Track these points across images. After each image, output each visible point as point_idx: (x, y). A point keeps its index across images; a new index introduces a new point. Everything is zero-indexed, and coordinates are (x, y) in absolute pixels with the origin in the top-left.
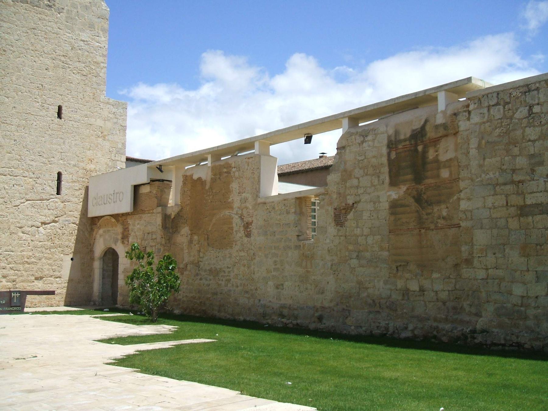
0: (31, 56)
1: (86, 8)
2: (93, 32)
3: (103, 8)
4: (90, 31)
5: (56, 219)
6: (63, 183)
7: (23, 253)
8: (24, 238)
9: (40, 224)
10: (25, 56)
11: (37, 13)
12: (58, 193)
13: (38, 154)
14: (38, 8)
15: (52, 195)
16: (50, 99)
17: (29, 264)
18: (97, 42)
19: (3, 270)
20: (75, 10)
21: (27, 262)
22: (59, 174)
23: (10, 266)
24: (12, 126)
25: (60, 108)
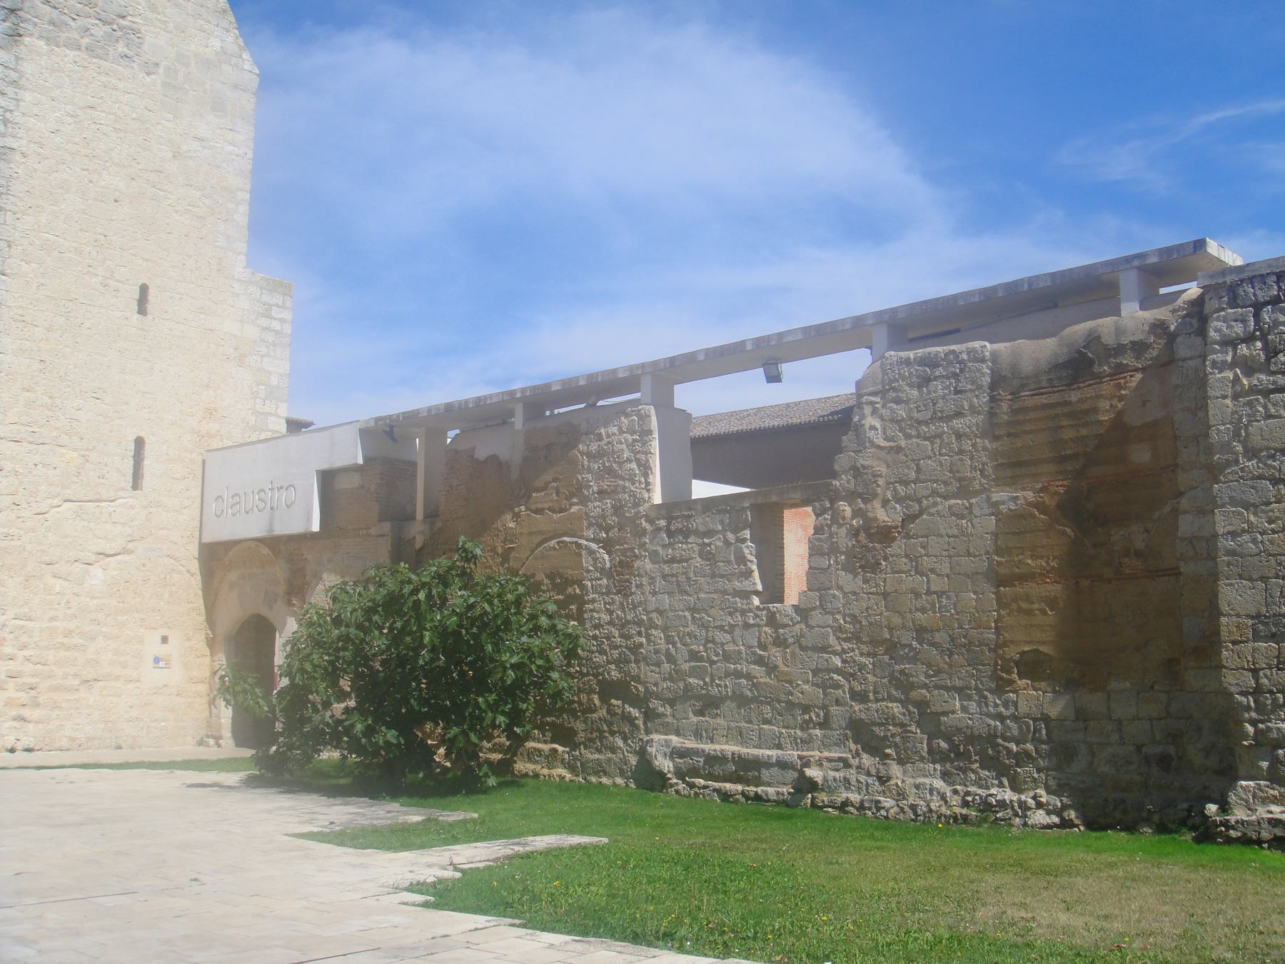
0: (84, 170)
5: (130, 546)
6: (146, 462)
7: (54, 623)
8: (57, 589)
9: (93, 557)
10: (71, 169)
12: (136, 485)
13: (95, 395)
14: (102, 62)
16: (123, 269)
17: (68, 649)
19: (7, 662)
21: (63, 644)
22: (140, 443)
23: (27, 653)
24: (36, 329)
25: (144, 289)
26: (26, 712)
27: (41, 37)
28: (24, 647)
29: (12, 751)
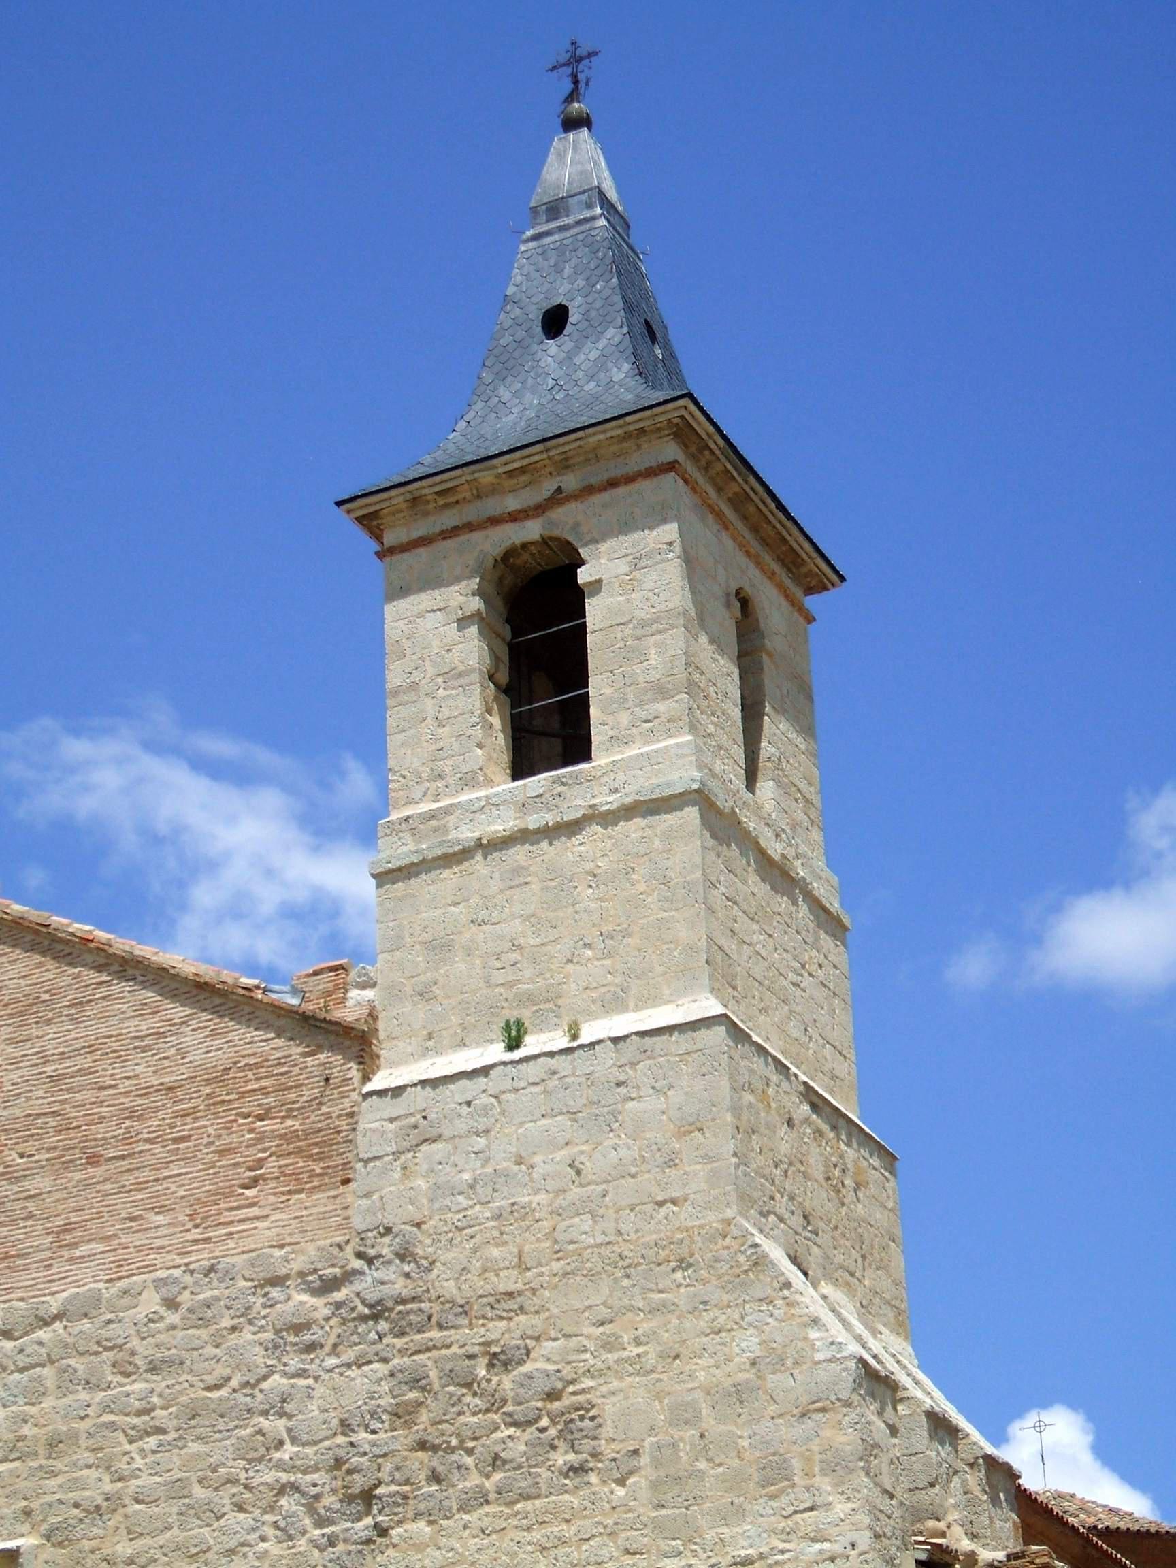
1: (740, 1393)
2: (784, 1500)
3: (819, 1356)
4: (772, 1497)
11: (529, 1529)
18: (814, 1540)
20: (693, 1432)
27: (418, 1515)
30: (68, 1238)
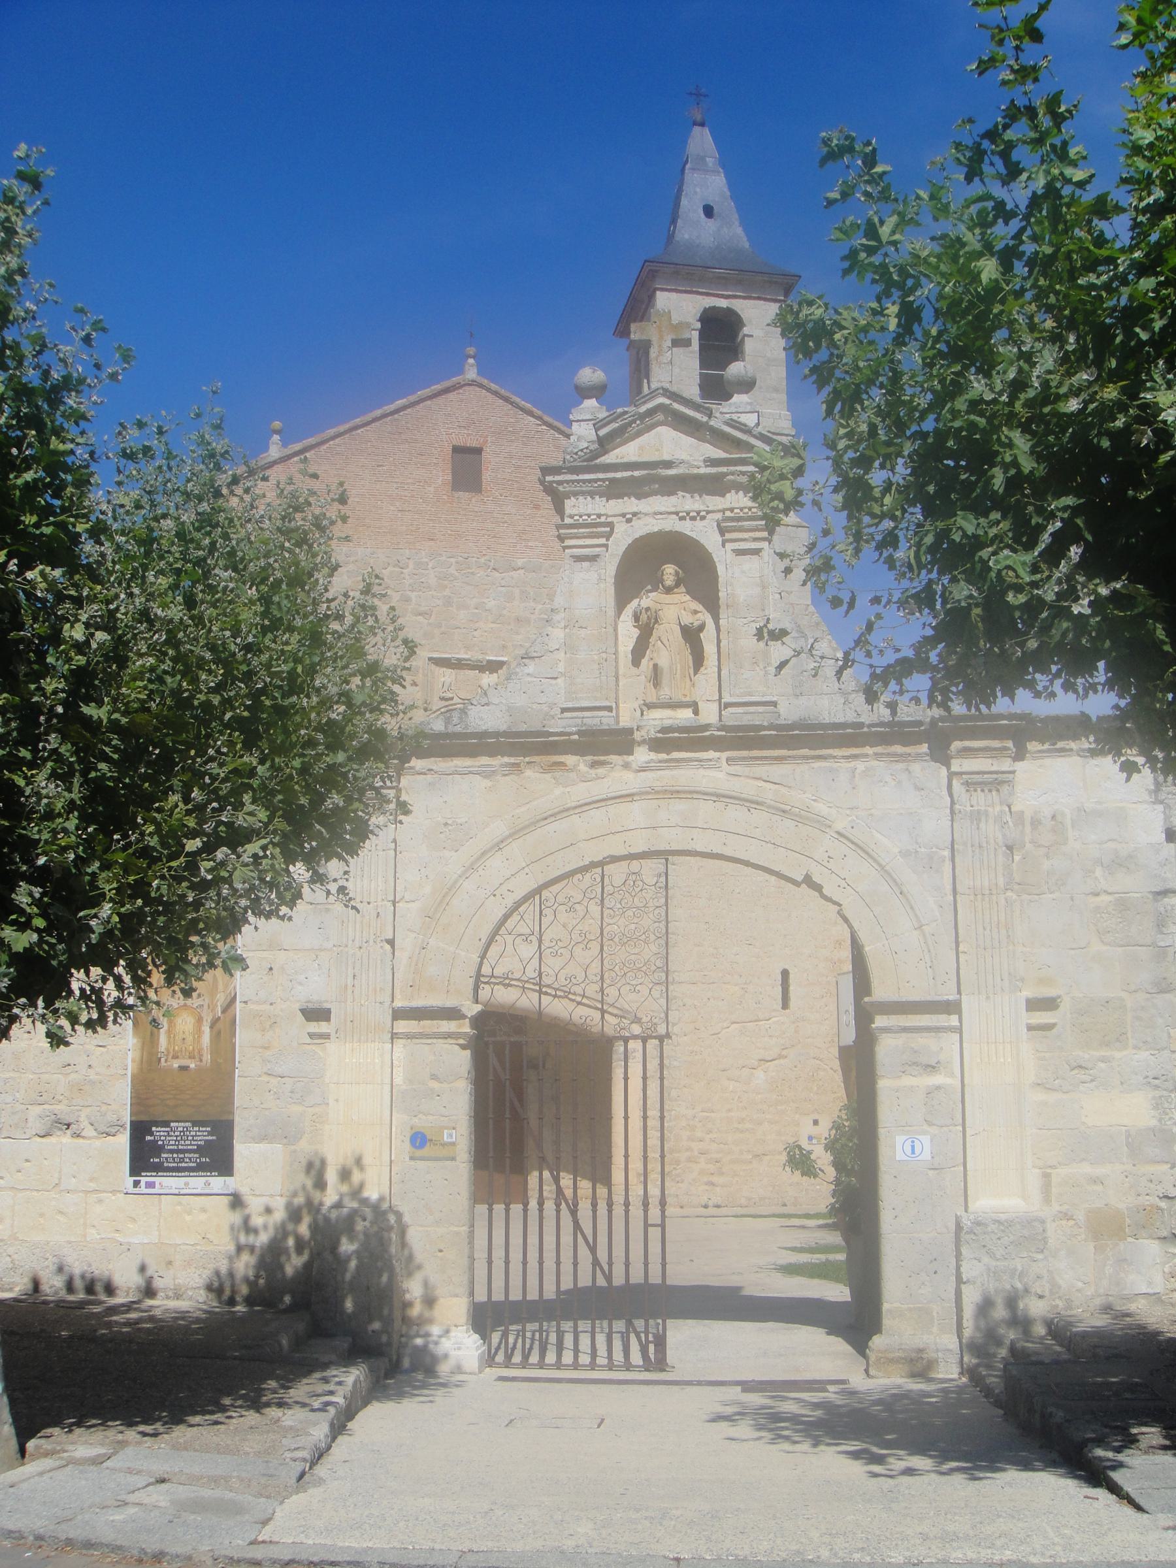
6: (791, 988)
12: (785, 1004)
15: (774, 1010)
17: (742, 1132)
22: (785, 974)
26: (715, 1179)
28: (710, 1132)
29: (706, 1207)
30: (524, 537)
